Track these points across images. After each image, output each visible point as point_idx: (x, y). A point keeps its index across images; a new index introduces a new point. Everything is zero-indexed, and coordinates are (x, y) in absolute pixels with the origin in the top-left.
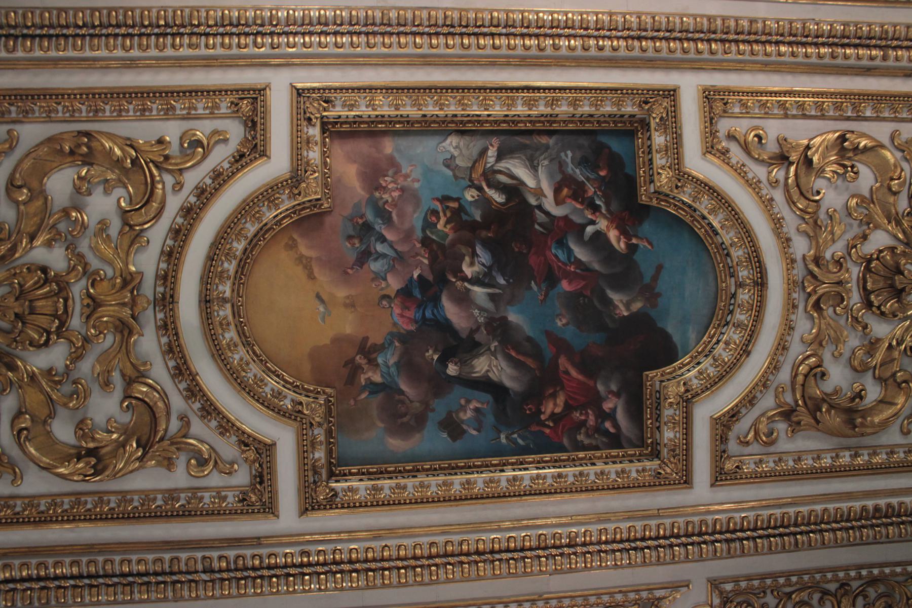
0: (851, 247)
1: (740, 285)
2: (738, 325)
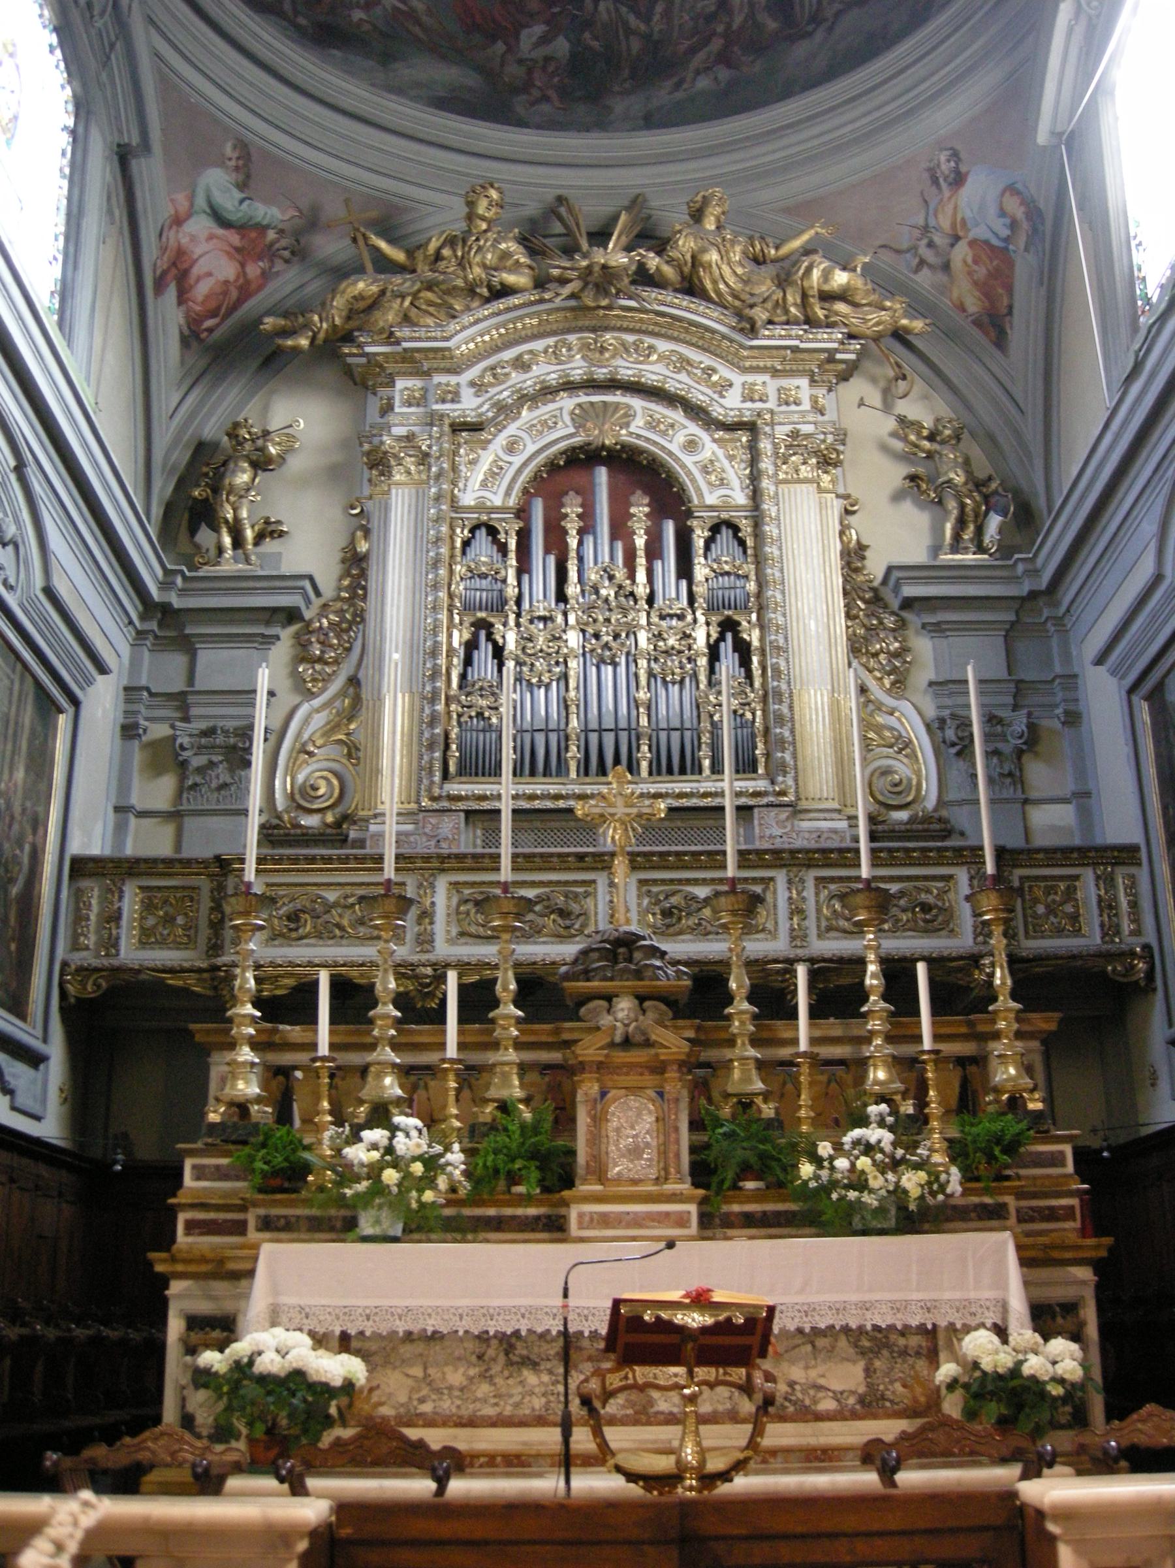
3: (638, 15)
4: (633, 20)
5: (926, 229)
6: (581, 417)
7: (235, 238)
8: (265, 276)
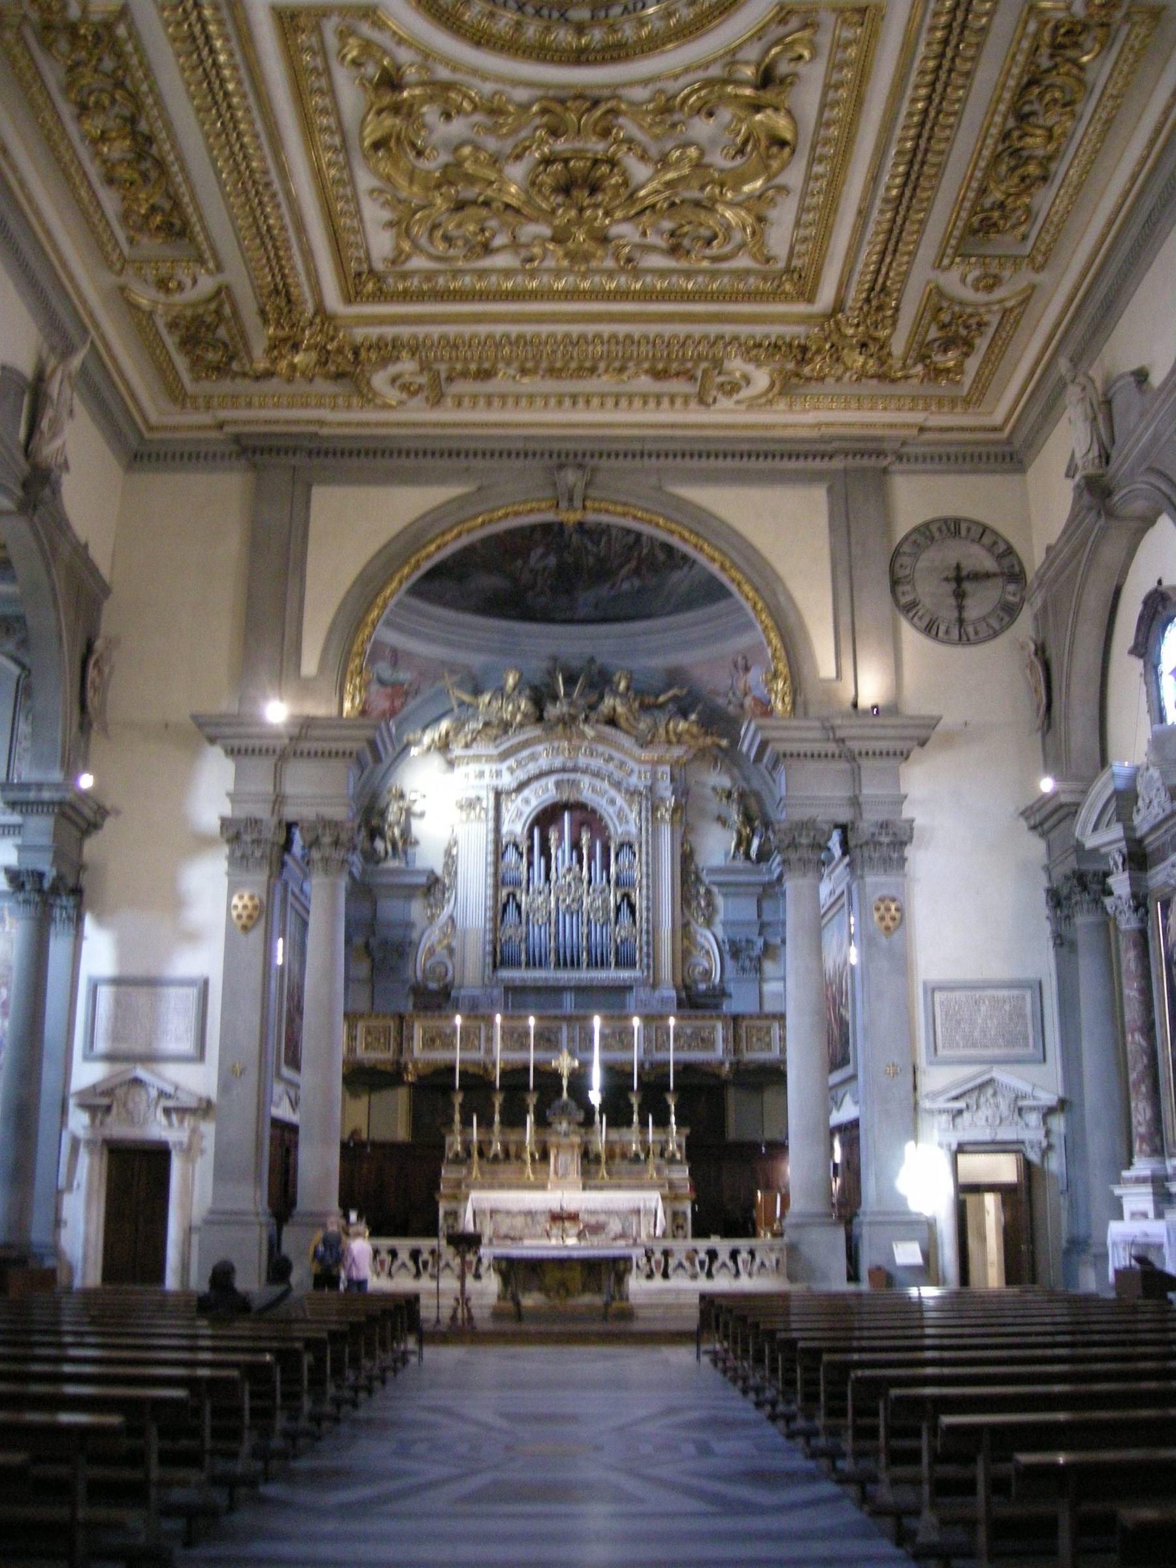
0: (629, 141)
1: (580, 29)
2: (518, 25)
3: (592, 541)
4: (589, 545)
5: (732, 687)
6: (558, 785)
7: (389, 690)
8: (403, 705)
